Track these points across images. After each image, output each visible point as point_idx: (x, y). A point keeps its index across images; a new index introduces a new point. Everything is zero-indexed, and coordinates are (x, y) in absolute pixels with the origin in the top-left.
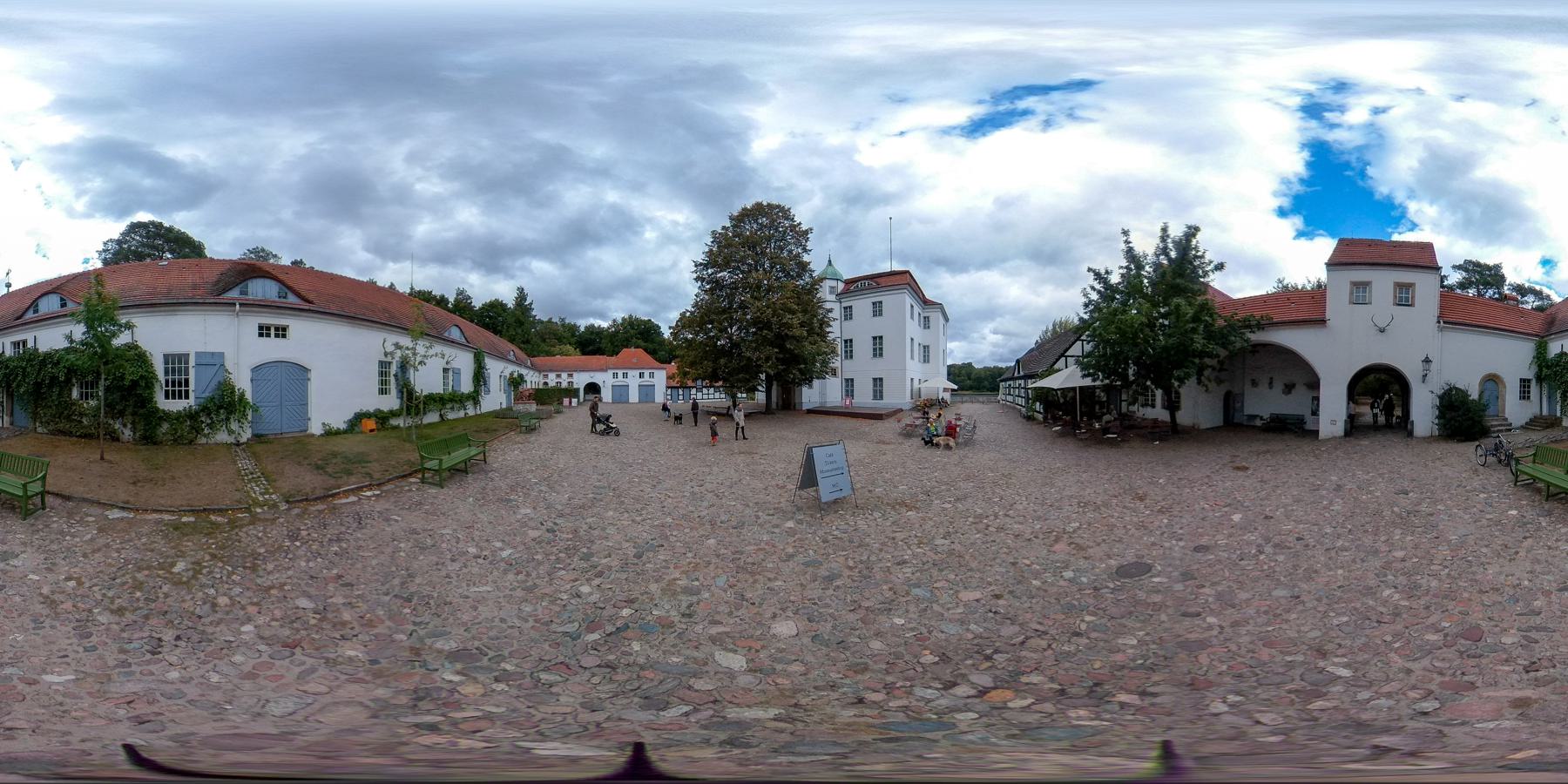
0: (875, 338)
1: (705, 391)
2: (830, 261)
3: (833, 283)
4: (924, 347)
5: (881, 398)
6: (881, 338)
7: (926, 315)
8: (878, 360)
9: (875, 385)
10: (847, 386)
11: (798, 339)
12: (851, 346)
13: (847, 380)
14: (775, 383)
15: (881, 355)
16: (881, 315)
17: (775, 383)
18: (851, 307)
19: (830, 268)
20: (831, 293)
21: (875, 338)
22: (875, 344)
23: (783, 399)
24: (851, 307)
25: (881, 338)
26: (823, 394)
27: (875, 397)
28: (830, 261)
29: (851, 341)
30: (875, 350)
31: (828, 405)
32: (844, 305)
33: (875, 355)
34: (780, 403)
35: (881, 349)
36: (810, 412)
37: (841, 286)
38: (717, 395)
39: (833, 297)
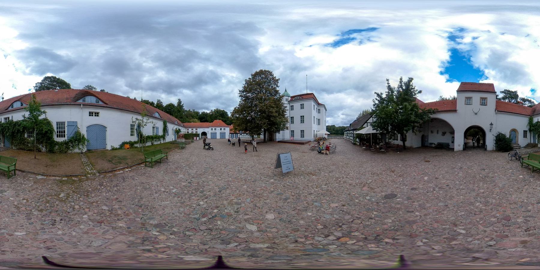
0: (301, 116)
1: (243, 135)
2: (286, 90)
3: (287, 98)
4: (318, 119)
5: (304, 137)
6: (303, 116)
7: (319, 108)
8: (302, 124)
9: (301, 133)
10: (292, 133)
11: (275, 117)
12: (293, 119)
13: (292, 131)
14: (267, 132)
15: (303, 122)
16: (303, 108)
17: (267, 132)
18: (293, 106)
19: (286, 92)
20: (286, 101)
21: (301, 116)
22: (301, 119)
23: (270, 138)
24: (293, 106)
25: (303, 116)
26: (283, 136)
27: (301, 137)
28: (286, 90)
29: (293, 117)
30: (301, 120)
31: (285, 139)
32: (291, 105)
33: (301, 122)
34: (269, 139)
35: (303, 120)
36: (279, 142)
37: (290, 99)
38: (247, 136)
39: (287, 102)
